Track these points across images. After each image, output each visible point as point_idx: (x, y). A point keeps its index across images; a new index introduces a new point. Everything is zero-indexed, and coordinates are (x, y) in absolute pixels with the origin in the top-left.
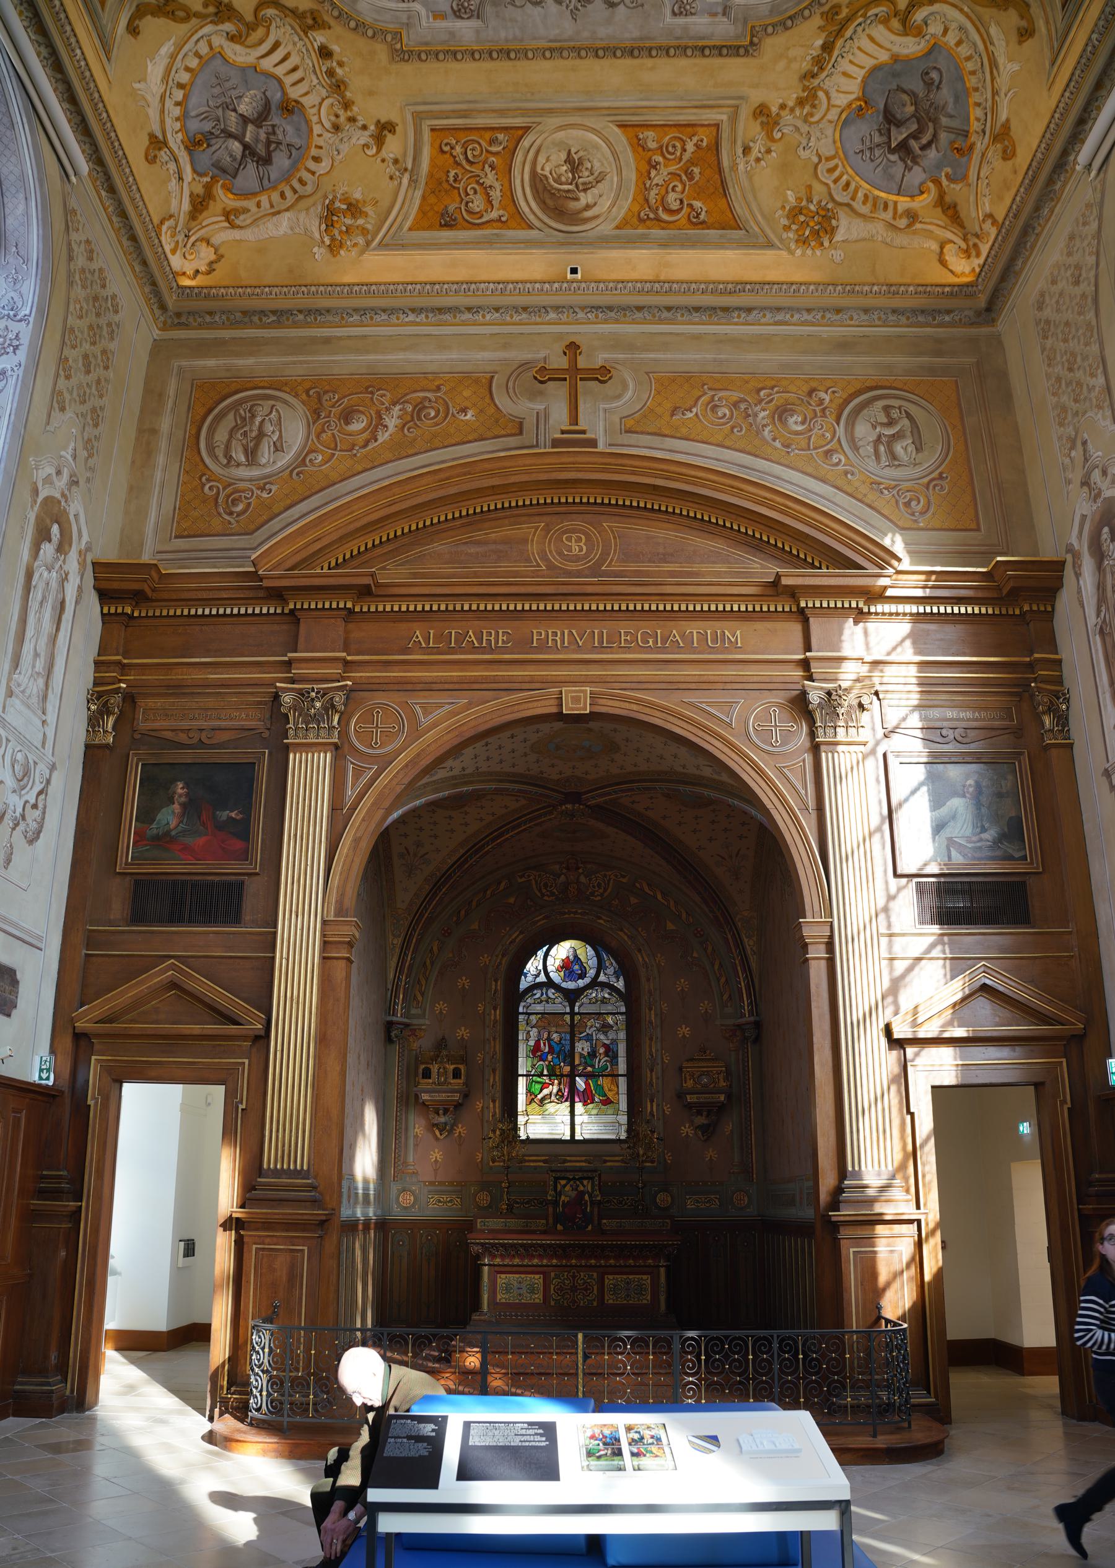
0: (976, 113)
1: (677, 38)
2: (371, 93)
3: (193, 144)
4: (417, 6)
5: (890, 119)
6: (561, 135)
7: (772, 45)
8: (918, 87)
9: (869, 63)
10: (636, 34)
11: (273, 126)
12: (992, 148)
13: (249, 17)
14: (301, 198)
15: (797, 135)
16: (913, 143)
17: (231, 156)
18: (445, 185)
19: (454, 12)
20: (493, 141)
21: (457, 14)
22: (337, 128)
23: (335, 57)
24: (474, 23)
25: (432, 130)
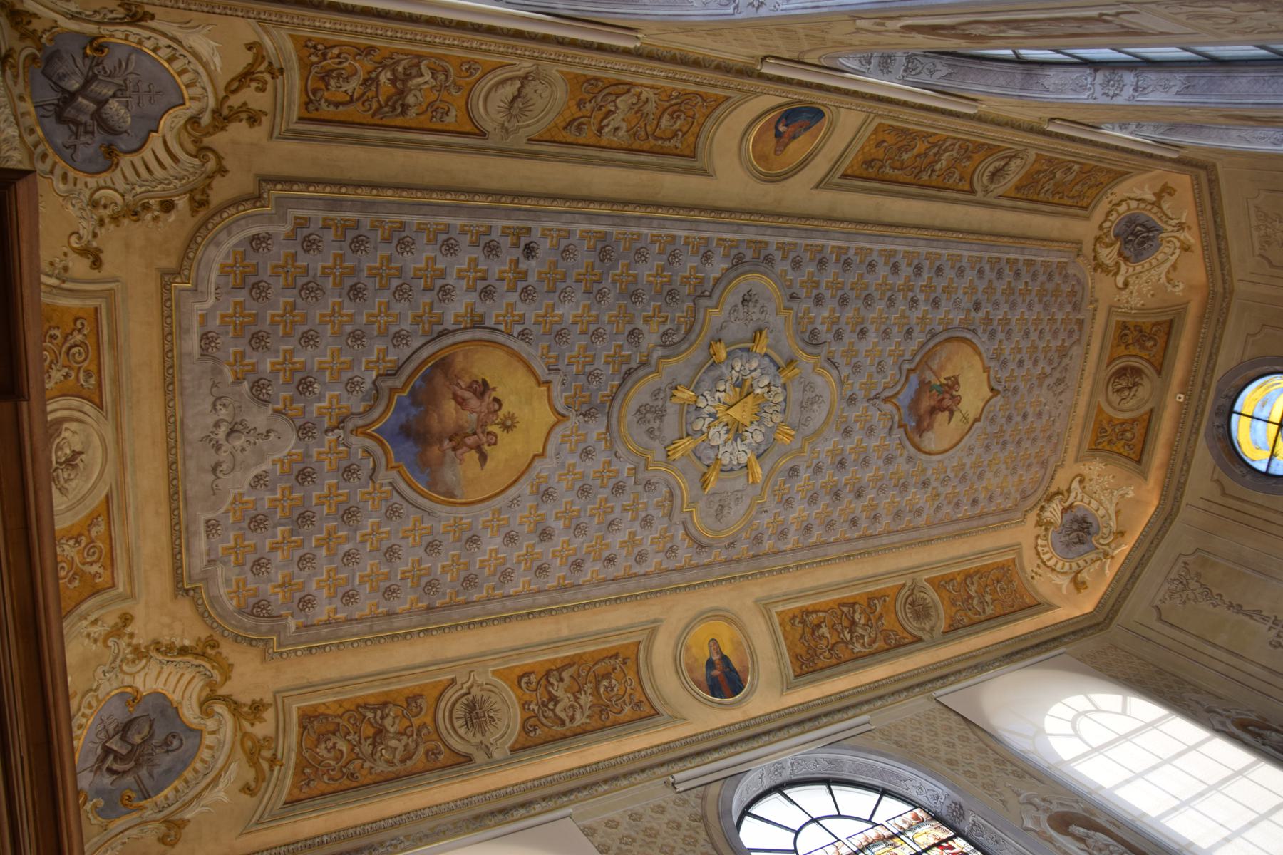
0: (168, 791)
1: (187, 528)
4: (211, 301)
5: (125, 729)
6: (96, 441)
7: (185, 608)
10: (190, 494)
11: (93, 133)
12: (157, 825)
13: (207, 141)
18: (47, 326)
19: (206, 334)
21: (205, 337)
22: (95, 204)
23: (163, 216)
24: (196, 351)
25: (96, 309)
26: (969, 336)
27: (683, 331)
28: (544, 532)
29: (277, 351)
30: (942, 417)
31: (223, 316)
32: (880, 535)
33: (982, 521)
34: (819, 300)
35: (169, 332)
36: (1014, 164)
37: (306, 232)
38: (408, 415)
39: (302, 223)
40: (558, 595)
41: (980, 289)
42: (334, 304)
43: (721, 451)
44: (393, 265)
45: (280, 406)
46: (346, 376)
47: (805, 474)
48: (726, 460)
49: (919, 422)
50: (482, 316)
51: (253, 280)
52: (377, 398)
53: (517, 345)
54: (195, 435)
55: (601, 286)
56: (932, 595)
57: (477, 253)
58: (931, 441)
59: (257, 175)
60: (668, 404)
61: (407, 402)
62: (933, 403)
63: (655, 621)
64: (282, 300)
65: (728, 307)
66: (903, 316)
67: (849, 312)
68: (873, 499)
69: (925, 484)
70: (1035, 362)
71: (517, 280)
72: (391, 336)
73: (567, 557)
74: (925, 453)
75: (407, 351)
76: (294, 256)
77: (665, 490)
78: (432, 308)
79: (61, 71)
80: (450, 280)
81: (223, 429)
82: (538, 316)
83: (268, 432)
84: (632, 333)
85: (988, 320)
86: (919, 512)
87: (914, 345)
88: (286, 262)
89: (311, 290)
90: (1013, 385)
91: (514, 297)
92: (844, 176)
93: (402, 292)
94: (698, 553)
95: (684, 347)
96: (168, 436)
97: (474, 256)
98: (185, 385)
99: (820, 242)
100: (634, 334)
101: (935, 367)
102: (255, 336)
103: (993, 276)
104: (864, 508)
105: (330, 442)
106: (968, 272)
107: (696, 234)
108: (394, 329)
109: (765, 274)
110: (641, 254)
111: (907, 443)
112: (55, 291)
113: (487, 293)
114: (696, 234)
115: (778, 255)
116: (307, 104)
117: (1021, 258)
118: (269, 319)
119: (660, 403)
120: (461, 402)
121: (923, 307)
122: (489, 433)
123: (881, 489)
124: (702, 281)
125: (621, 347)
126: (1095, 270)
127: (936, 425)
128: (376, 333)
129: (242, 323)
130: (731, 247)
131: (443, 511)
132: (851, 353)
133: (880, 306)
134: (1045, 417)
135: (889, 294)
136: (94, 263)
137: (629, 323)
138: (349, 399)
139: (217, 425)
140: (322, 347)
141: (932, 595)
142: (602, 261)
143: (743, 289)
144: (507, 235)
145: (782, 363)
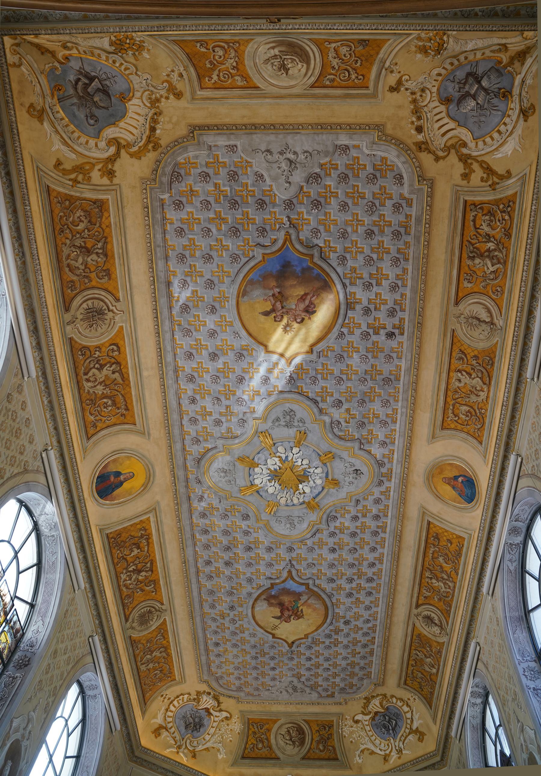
2: (399, 107)
3: (506, 94)
4: (367, 152)
8: (98, 112)
9: (128, 120)
14: (454, 57)
15: (155, 84)
16: (87, 81)
17: (490, 78)
18: (363, 58)
19: (349, 149)
20: (333, 80)
21: (347, 147)
24: (339, 143)
25: (368, 87)
26: (328, 621)
27: (340, 434)
28: (216, 355)
29: (337, 189)
30: (277, 611)
31: (358, 158)
32: (199, 582)
33: (203, 652)
34: (355, 518)
35: (351, 128)
36: (436, 630)
37: (404, 205)
38: (296, 266)
39: (409, 203)
40: (171, 368)
41: (357, 623)
42: (364, 221)
43: (263, 467)
44: (385, 255)
45: (305, 189)
46: (321, 228)
47: (244, 525)
48: (256, 470)
49: (274, 597)
50: (354, 309)
51: (378, 175)
52: (307, 247)
53: (335, 332)
54: (290, 140)
55: (369, 380)
56: (154, 625)
57: (390, 304)
58: (262, 607)
59: (435, 178)
60: (295, 429)
61: (304, 265)
62: (286, 604)
63: (149, 434)
64: (367, 191)
65: (353, 460)
66: (342, 575)
67: (346, 539)
68: (224, 574)
69: (232, 608)
70: (309, 669)
71: (374, 328)
72: (344, 254)
73: (198, 372)
74: (253, 604)
75: (334, 264)
76: (391, 198)
77: (239, 433)
78: (359, 278)
79: (492, 77)
80: (375, 289)
81: (293, 156)
82: (353, 343)
83: (290, 183)
84: (340, 402)
85: (337, 631)
86: (213, 606)
87: (324, 585)
88: (388, 194)
89: (371, 208)
90: (295, 657)
91: (364, 327)
92: (429, 523)
93: (369, 261)
94: (194, 459)
95: (330, 435)
96: (291, 124)
97: (389, 302)
98: (320, 135)
99: (390, 514)
100: (339, 404)
101: (310, 601)
102: (347, 176)
103: (365, 630)
104: (217, 569)
105: (282, 219)
106: (369, 612)
107: (397, 436)
108: (348, 256)
109: (372, 482)
110: (386, 403)
111: (260, 591)
112: (382, 64)
113: (367, 311)
114: (397, 436)
115: (383, 489)
116: (474, 204)
117: (375, 647)
118: (356, 184)
119: (296, 424)
120: (302, 298)
121: (348, 586)
122: (282, 316)
123: (230, 578)
124: (369, 442)
125: (332, 395)
126: (365, 698)
127: (272, 608)
128: (346, 245)
129: (354, 168)
130: (389, 458)
131: (234, 290)
132: (321, 544)
133: (350, 559)
134: (272, 683)
135: (356, 563)
136: (393, 88)
137: (346, 399)
138: (308, 230)
139: (295, 153)
140: (339, 214)
141: (154, 625)
142: (383, 380)
143: (364, 469)
144: (400, 322)
145: (317, 500)
